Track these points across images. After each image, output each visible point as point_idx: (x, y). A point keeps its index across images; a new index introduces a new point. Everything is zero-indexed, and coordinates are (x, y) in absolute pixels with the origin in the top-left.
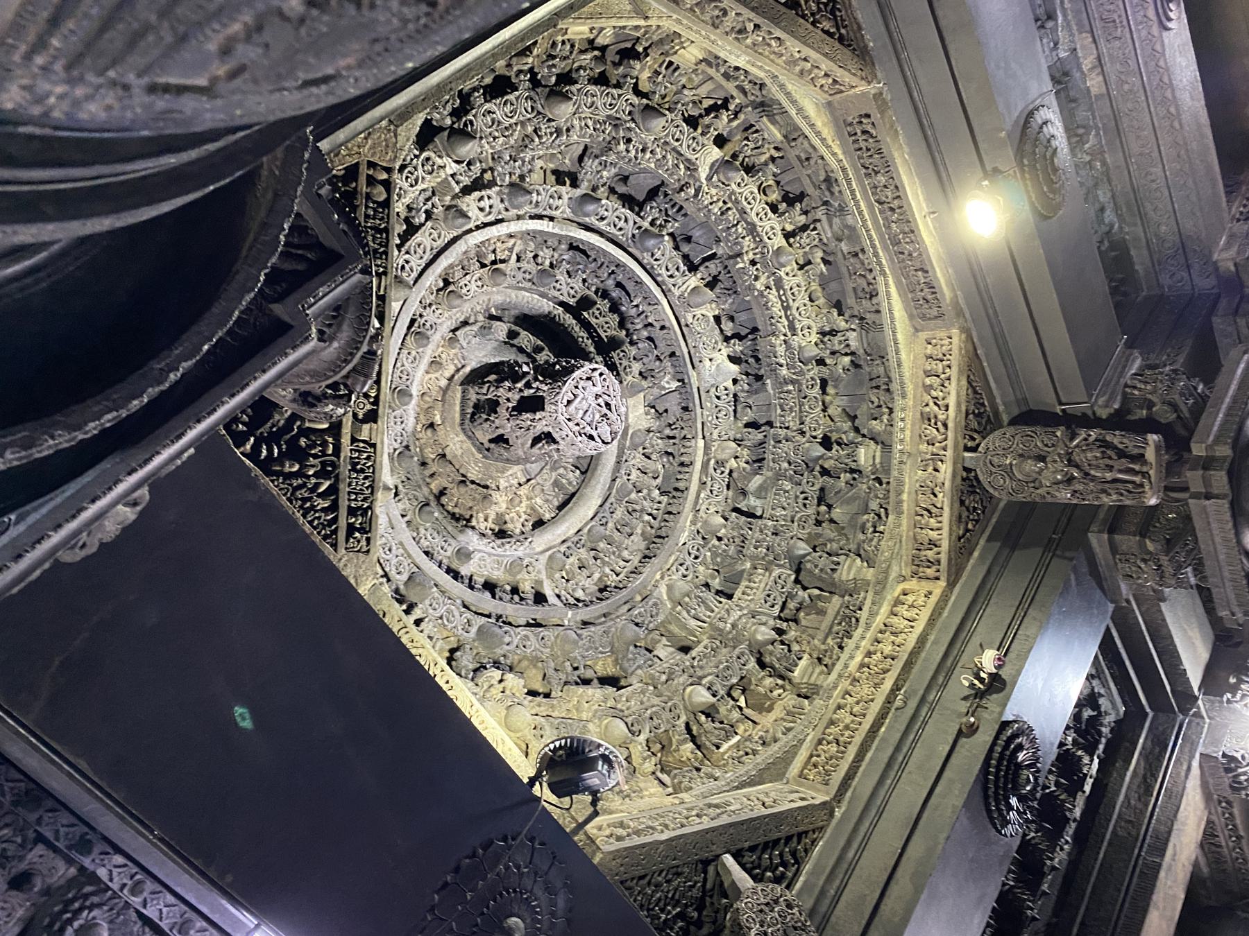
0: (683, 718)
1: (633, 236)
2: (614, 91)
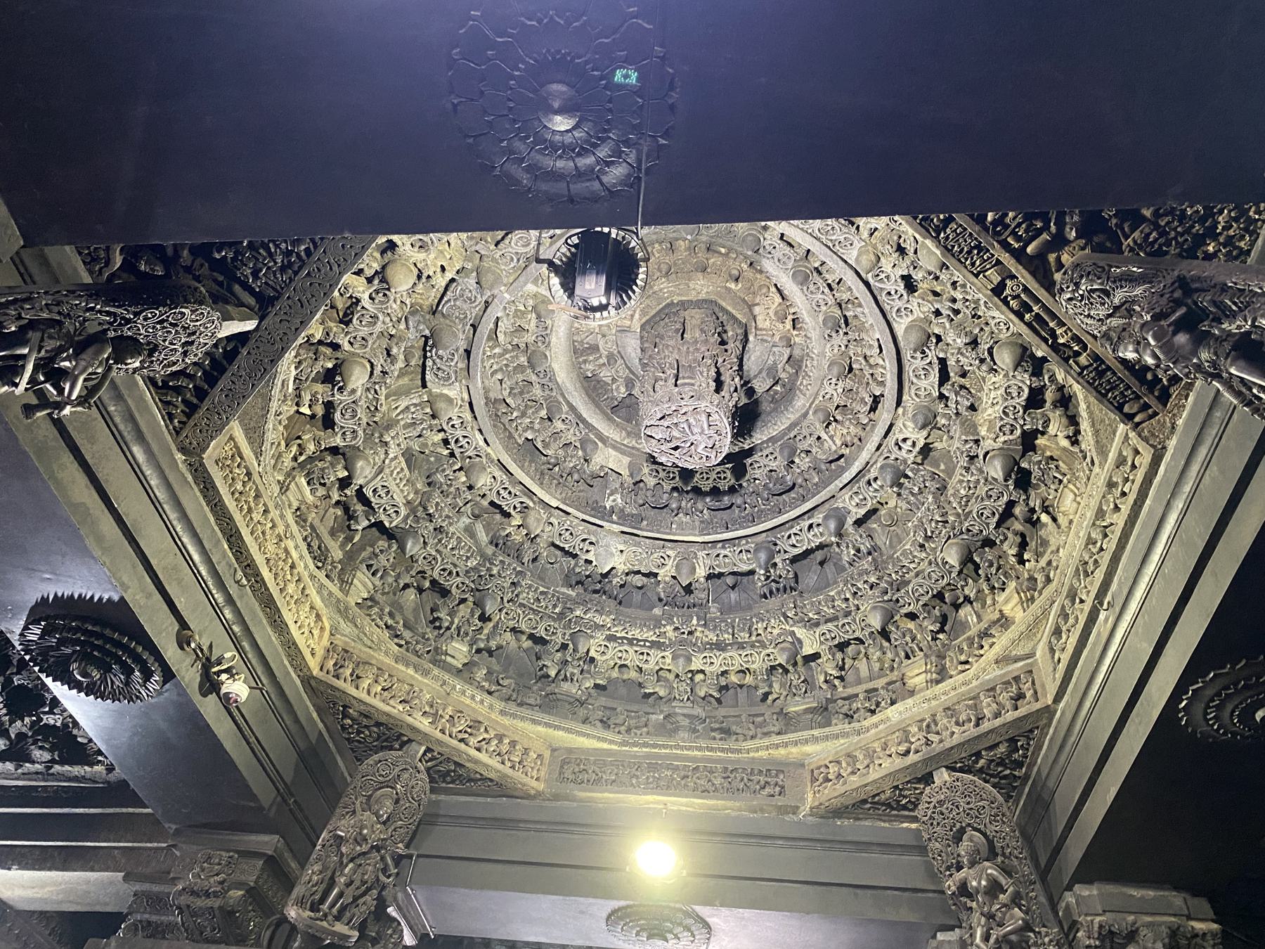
0: (347, 347)
1: (776, 544)
2: (925, 599)
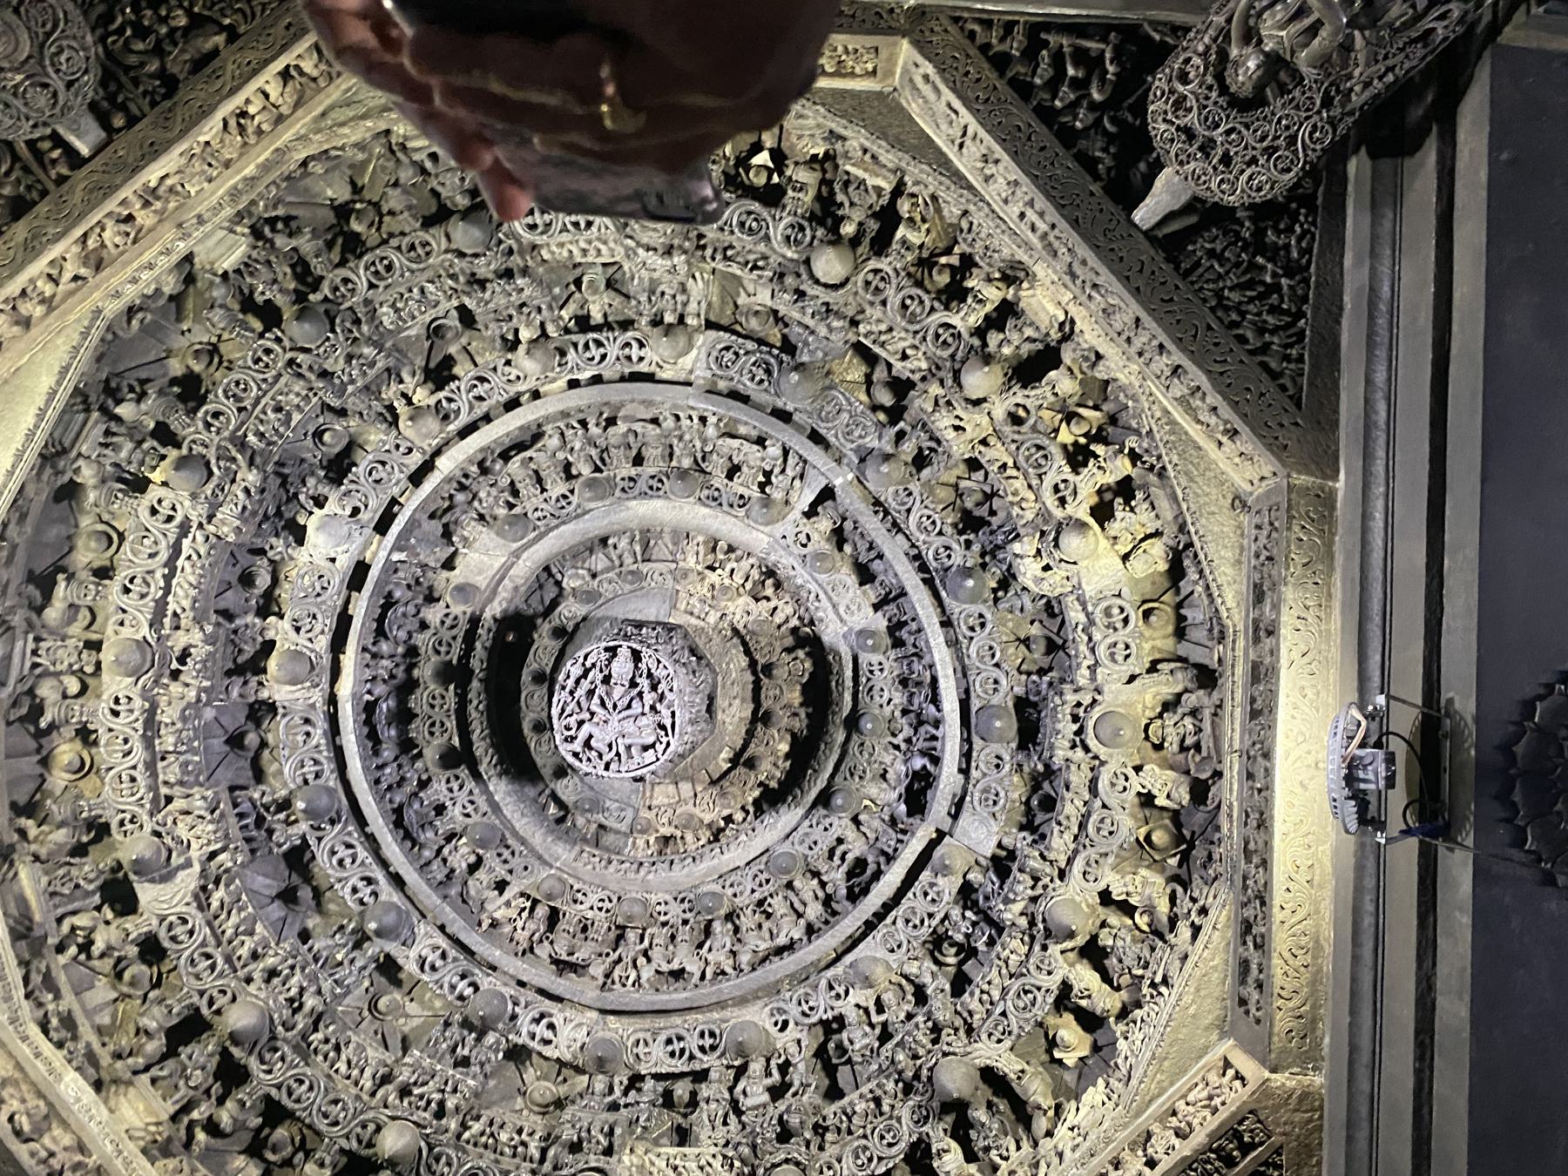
1: (332, 822)
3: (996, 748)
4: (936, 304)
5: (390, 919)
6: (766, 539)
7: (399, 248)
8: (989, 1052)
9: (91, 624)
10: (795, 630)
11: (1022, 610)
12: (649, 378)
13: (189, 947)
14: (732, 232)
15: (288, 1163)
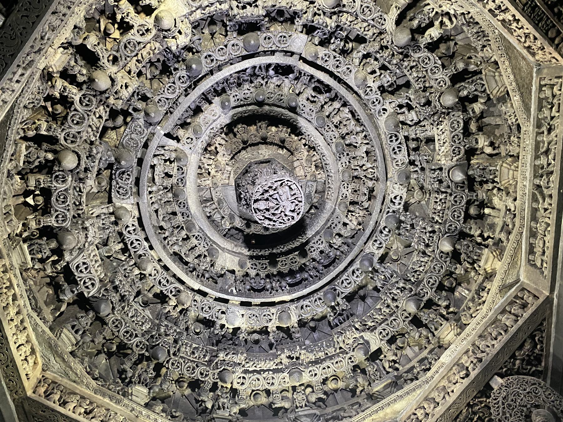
1: (335, 290)
3: (262, 41)
4: (72, 109)
5: (366, 263)
6: (193, 155)
7: (118, 331)
8: (390, 24)
9: (286, 390)
10: (226, 134)
11: (200, 39)
12: (140, 220)
13: (388, 329)
14: (68, 205)
15: (455, 279)
